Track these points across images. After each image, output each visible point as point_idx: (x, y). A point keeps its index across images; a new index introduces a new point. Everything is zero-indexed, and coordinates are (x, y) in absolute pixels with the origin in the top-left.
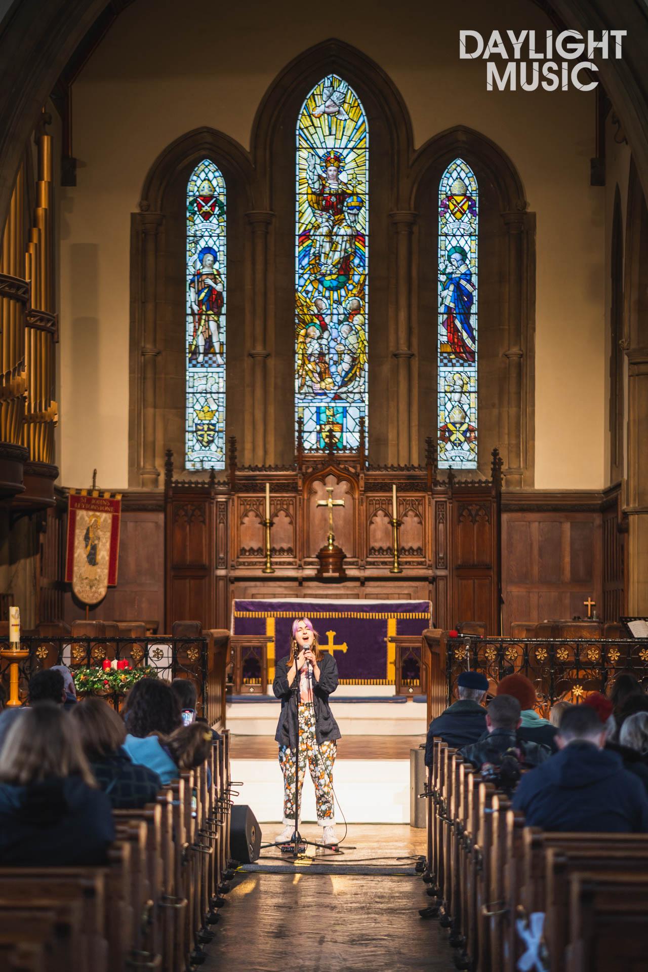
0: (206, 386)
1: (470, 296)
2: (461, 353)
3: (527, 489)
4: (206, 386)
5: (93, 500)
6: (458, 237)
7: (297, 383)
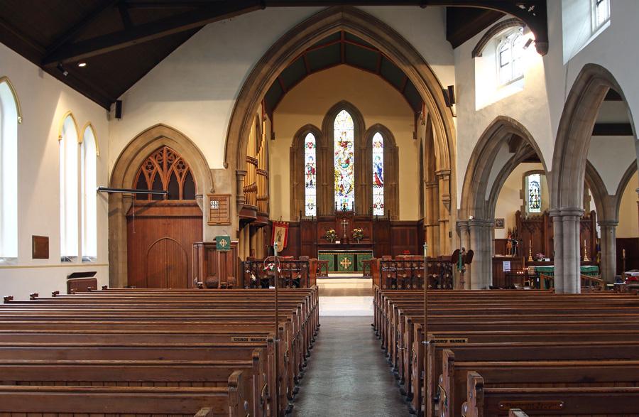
0: (311, 194)
2: (380, 185)
4: (311, 194)
5: (280, 224)
6: (378, 155)
7: (335, 192)
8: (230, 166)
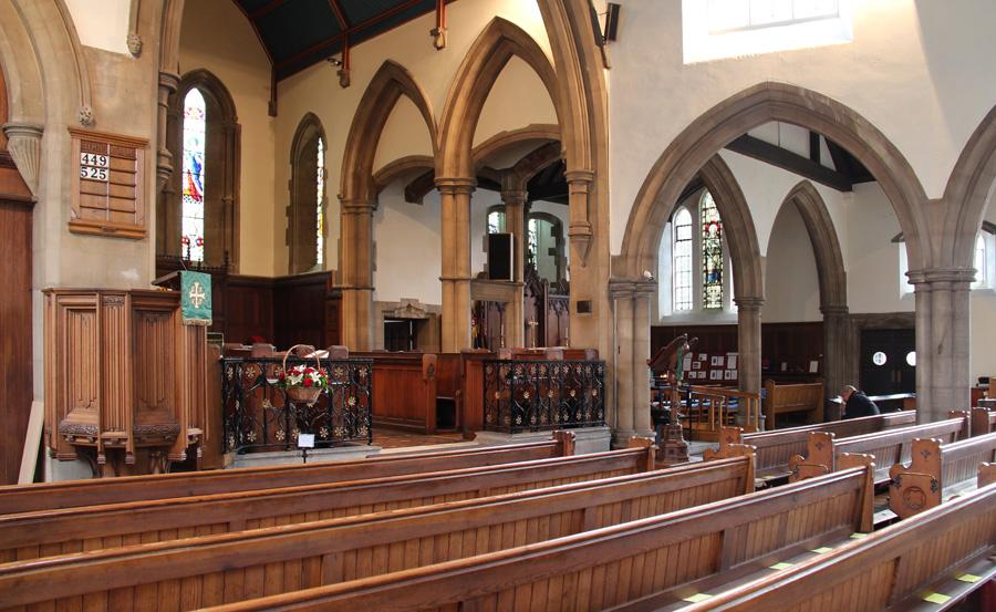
1: (200, 166)
2: (196, 196)
3: (236, 274)
8: (148, 54)
